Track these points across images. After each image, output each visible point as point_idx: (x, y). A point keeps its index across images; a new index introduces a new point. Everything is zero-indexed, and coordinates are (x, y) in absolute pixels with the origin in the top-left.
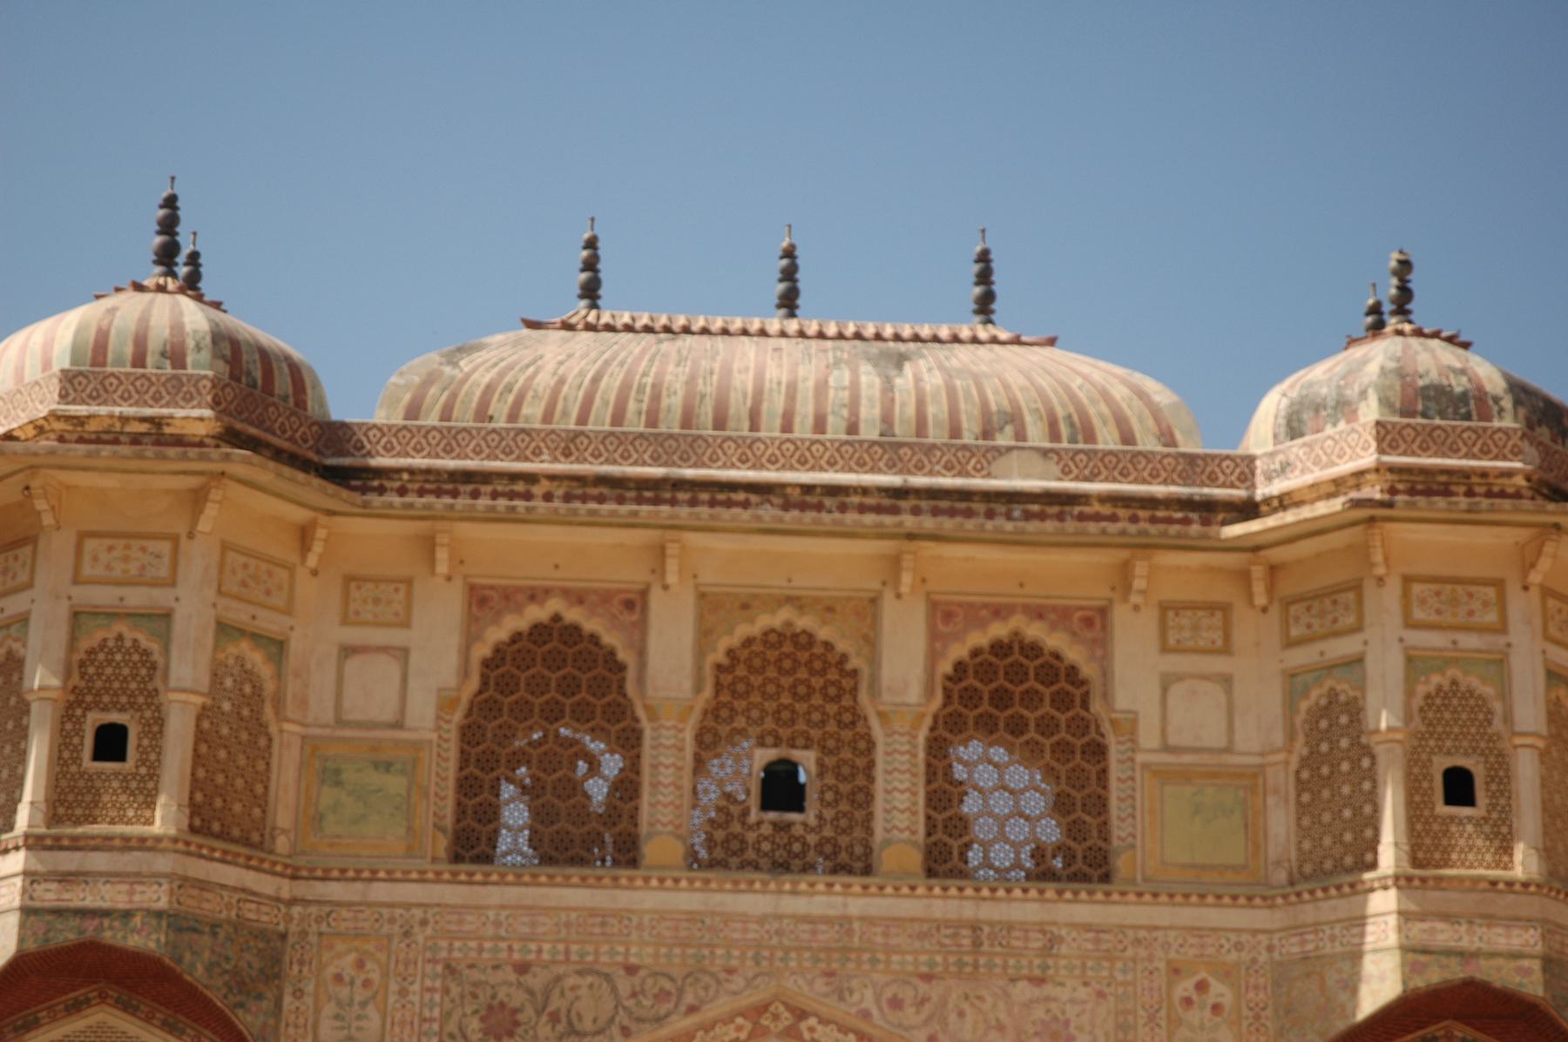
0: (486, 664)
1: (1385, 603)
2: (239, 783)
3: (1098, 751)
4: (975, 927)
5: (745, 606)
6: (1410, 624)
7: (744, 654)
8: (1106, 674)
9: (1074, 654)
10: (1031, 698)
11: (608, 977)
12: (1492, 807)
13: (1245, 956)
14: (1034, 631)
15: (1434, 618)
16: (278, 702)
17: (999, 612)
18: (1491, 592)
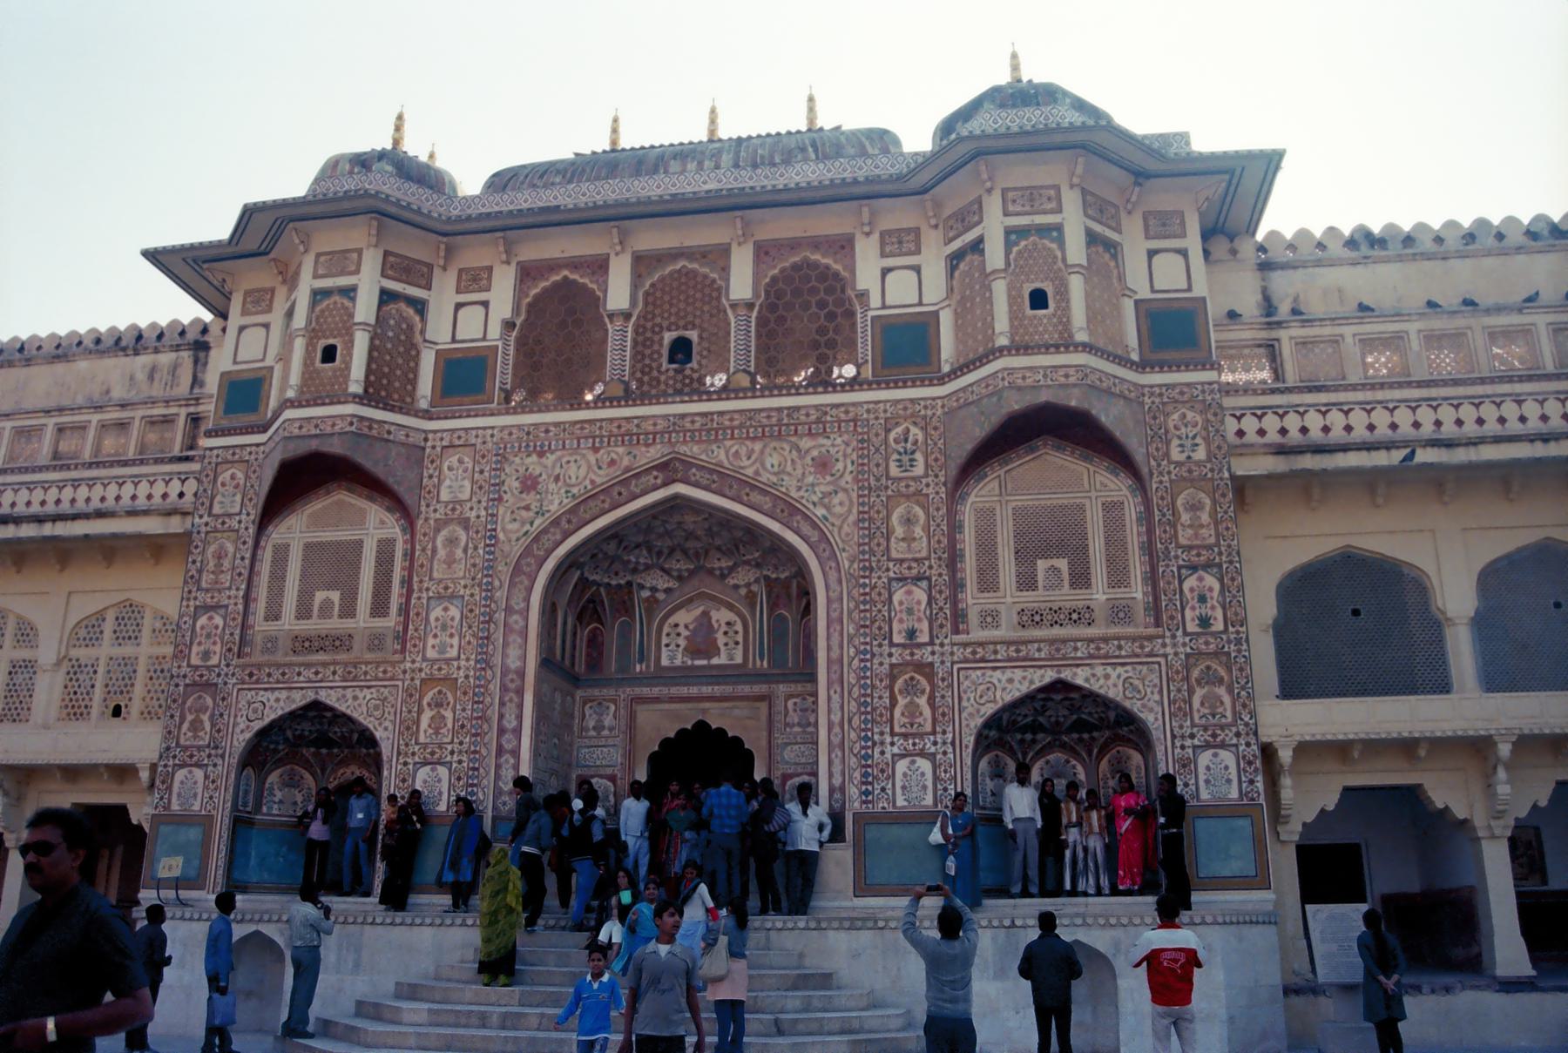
0: (530, 305)
1: (993, 206)
2: (398, 372)
3: (851, 314)
4: (779, 410)
5: (659, 261)
6: (1006, 214)
7: (660, 286)
8: (853, 272)
9: (837, 267)
10: (813, 291)
11: (584, 456)
12: (1058, 308)
13: (929, 413)
14: (816, 257)
15: (1019, 209)
16: (423, 332)
17: (794, 245)
18: (1052, 192)
